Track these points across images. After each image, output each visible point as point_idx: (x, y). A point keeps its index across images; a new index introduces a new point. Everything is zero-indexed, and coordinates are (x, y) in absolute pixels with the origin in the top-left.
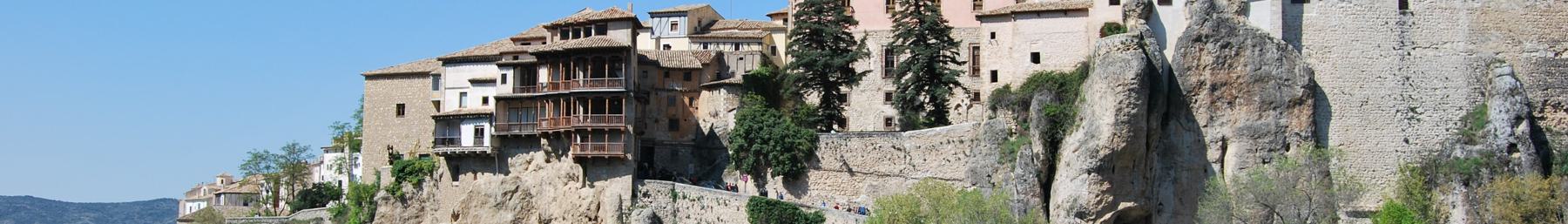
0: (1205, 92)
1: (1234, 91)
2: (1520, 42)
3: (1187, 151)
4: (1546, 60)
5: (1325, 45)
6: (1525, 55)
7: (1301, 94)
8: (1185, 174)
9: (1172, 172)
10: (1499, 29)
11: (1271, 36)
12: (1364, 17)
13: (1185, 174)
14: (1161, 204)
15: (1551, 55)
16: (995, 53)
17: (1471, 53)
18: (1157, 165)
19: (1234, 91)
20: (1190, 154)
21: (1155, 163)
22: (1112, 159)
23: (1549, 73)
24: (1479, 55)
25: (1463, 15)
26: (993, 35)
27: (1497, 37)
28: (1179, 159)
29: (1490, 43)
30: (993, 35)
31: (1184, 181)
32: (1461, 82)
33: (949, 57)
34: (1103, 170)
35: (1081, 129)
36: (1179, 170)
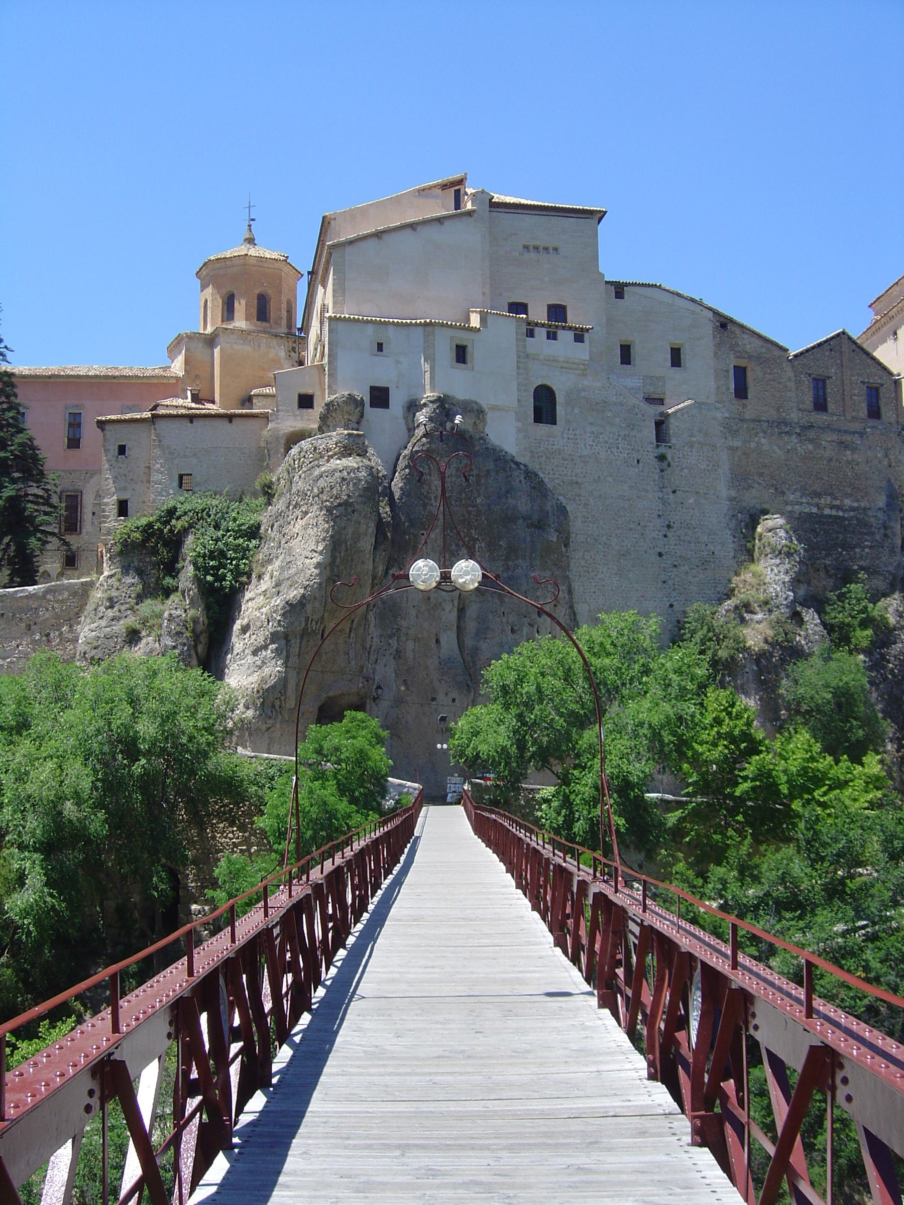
0: (437, 530)
1: (473, 532)
2: (783, 493)
3: (413, 612)
4: (810, 514)
5: (574, 478)
6: (789, 508)
7: (555, 539)
8: (410, 645)
9: (394, 642)
10: (761, 475)
11: (519, 459)
12: (618, 448)
13: (410, 645)
14: (379, 687)
15: (815, 510)
16: (125, 475)
17: (731, 499)
18: (374, 631)
19: (473, 532)
20: (417, 617)
21: (372, 628)
22: (322, 618)
23: (814, 531)
24: (744, 504)
25: (724, 456)
26: (122, 450)
27: (759, 483)
28: (404, 623)
29: (754, 491)
30: (122, 450)
31: (410, 655)
32: (727, 535)
33: (41, 497)
34: (309, 634)
35: (267, 577)
36: (404, 639)
